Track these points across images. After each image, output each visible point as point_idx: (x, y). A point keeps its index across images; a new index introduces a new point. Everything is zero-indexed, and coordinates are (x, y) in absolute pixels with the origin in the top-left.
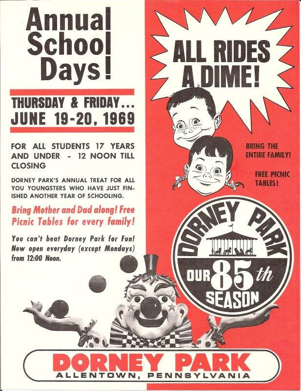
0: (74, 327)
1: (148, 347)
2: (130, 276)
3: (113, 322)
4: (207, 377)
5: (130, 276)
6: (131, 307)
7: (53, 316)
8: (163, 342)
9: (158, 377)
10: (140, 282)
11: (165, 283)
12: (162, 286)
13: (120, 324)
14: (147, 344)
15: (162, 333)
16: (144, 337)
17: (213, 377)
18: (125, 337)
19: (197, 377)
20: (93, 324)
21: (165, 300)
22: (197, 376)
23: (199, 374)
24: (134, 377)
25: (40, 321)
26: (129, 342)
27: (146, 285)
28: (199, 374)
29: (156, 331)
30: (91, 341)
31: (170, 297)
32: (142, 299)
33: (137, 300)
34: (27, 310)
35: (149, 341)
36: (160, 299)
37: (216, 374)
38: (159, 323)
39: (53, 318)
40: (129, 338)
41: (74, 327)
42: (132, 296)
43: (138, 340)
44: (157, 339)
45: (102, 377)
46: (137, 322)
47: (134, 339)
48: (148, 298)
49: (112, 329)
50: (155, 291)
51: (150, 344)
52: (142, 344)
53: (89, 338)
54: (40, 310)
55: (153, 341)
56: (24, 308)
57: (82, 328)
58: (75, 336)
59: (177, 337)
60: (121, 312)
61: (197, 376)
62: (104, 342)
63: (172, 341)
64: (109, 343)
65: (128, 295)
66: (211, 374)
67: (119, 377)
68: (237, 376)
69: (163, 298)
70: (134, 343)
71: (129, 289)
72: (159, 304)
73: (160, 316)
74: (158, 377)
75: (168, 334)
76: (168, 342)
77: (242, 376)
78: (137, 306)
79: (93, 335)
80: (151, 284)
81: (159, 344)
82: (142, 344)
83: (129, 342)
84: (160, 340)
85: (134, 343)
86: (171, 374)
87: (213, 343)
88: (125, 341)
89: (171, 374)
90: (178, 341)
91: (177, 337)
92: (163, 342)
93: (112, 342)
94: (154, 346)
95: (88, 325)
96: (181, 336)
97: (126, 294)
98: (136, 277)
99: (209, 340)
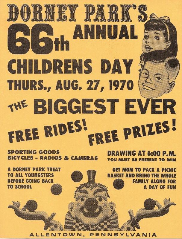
0: (41, 218)
1: (89, 230)
2: (78, 184)
3: (67, 214)
5: (78, 184)
6: (78, 205)
7: (27, 210)
8: (99, 227)
10: (84, 188)
11: (101, 188)
12: (99, 191)
13: (71, 216)
14: (88, 229)
15: (98, 222)
16: (87, 224)
18: (74, 224)
20: (53, 215)
21: (100, 200)
25: (19, 214)
26: (77, 227)
27: (88, 190)
29: (95, 220)
30: (52, 226)
31: (104, 197)
32: (86, 199)
33: (82, 200)
34: (10, 207)
35: (90, 226)
36: (97, 199)
38: (97, 215)
39: (27, 211)
40: (77, 224)
41: (41, 218)
42: (79, 197)
43: (83, 226)
44: (95, 225)
46: (82, 214)
47: (80, 225)
48: (89, 198)
49: (66, 219)
50: (94, 194)
51: (91, 228)
52: (86, 228)
53: (52, 224)
54: (18, 206)
55: (92, 226)
56: (8, 205)
57: (46, 218)
58: (42, 223)
59: (108, 224)
60: (72, 208)
62: (60, 228)
63: (105, 227)
64: (64, 227)
65: (77, 196)
69: (99, 199)
70: (80, 228)
71: (77, 192)
72: (97, 203)
73: (97, 210)
75: (102, 222)
76: (102, 227)
78: (82, 204)
79: (53, 222)
80: (91, 189)
81: (97, 228)
82: (85, 228)
83: (77, 227)
84: (97, 226)
85: (80, 228)
87: (132, 228)
88: (74, 227)
90: (109, 227)
91: (108, 224)
92: (99, 227)
93: (66, 227)
94: (94, 230)
95: (49, 216)
96: (111, 224)
97: (75, 196)
98: (82, 185)
99: (129, 226)
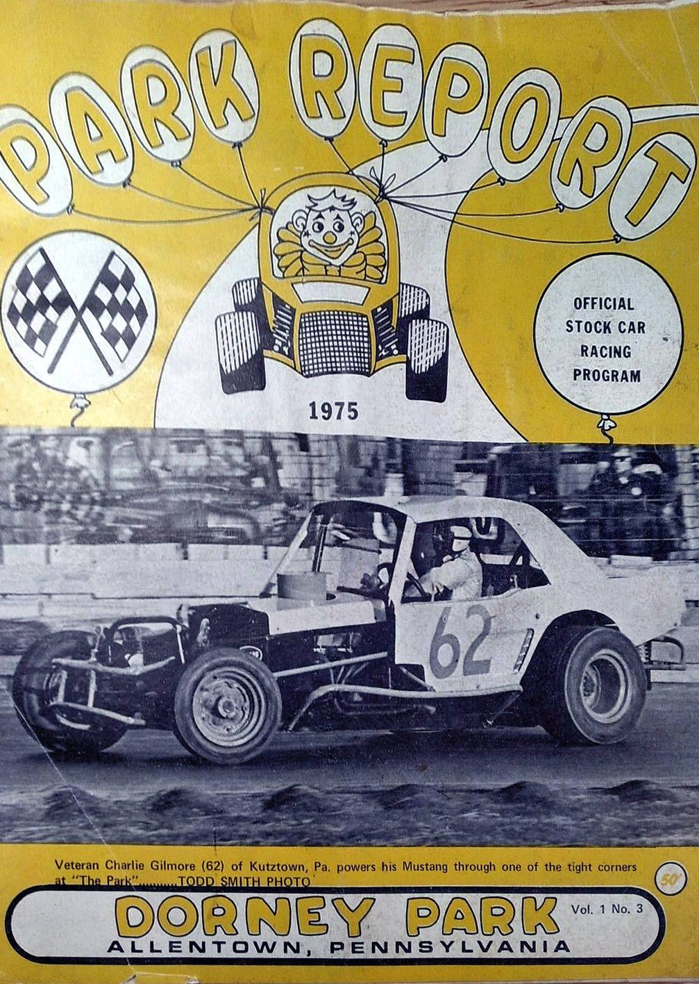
4: (471, 951)
9: (354, 952)
17: (485, 950)
19: (447, 951)
22: (447, 948)
23: (452, 942)
24: (297, 951)
28: (452, 942)
37: (491, 942)
45: (219, 951)
61: (447, 948)
66: (479, 943)
67: (260, 951)
68: (540, 947)
74: (354, 952)
77: (552, 945)
86: (386, 944)
89: (386, 944)
